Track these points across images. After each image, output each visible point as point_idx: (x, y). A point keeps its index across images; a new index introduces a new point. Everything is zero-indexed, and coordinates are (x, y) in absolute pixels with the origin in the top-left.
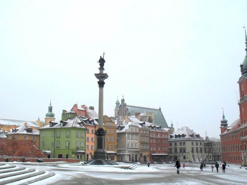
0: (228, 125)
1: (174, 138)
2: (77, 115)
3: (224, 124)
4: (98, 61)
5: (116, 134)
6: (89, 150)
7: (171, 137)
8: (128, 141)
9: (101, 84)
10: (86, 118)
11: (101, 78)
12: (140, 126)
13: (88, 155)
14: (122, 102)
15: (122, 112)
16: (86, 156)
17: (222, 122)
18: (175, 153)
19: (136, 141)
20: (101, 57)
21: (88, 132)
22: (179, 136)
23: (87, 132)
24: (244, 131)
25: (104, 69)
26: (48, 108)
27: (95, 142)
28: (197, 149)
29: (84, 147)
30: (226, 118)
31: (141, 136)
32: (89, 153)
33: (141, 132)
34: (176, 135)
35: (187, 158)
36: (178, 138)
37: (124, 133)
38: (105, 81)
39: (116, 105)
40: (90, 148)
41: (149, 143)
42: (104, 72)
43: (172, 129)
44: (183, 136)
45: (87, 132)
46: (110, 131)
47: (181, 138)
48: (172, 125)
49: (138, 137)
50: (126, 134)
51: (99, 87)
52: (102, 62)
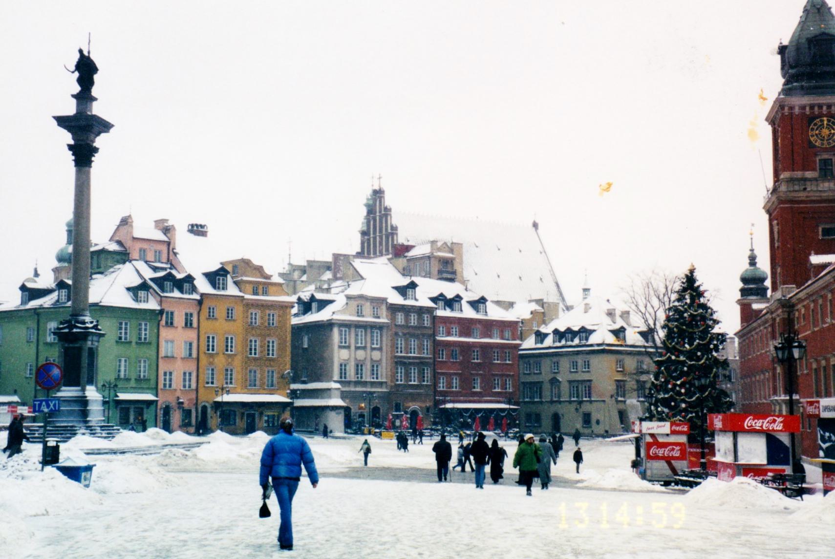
1: (549, 341)
2: (132, 256)
4: (73, 68)
5: (289, 330)
6: (175, 390)
8: (344, 354)
9: (83, 154)
11: (83, 132)
14: (375, 200)
16: (160, 413)
17: (744, 280)
18: (552, 402)
19: (376, 355)
20: (81, 51)
21: (170, 324)
22: (569, 334)
23: (163, 322)
25: (96, 99)
26: (66, 228)
29: (153, 377)
32: (174, 404)
33: (400, 318)
34: (556, 332)
35: (598, 422)
36: (563, 342)
37: (329, 325)
38: (100, 141)
41: (431, 361)
42: (97, 109)
44: (585, 332)
45: (163, 322)
46: (262, 318)
47: (576, 341)
49: (384, 339)
50: (331, 330)
51: (73, 163)
52: (86, 69)
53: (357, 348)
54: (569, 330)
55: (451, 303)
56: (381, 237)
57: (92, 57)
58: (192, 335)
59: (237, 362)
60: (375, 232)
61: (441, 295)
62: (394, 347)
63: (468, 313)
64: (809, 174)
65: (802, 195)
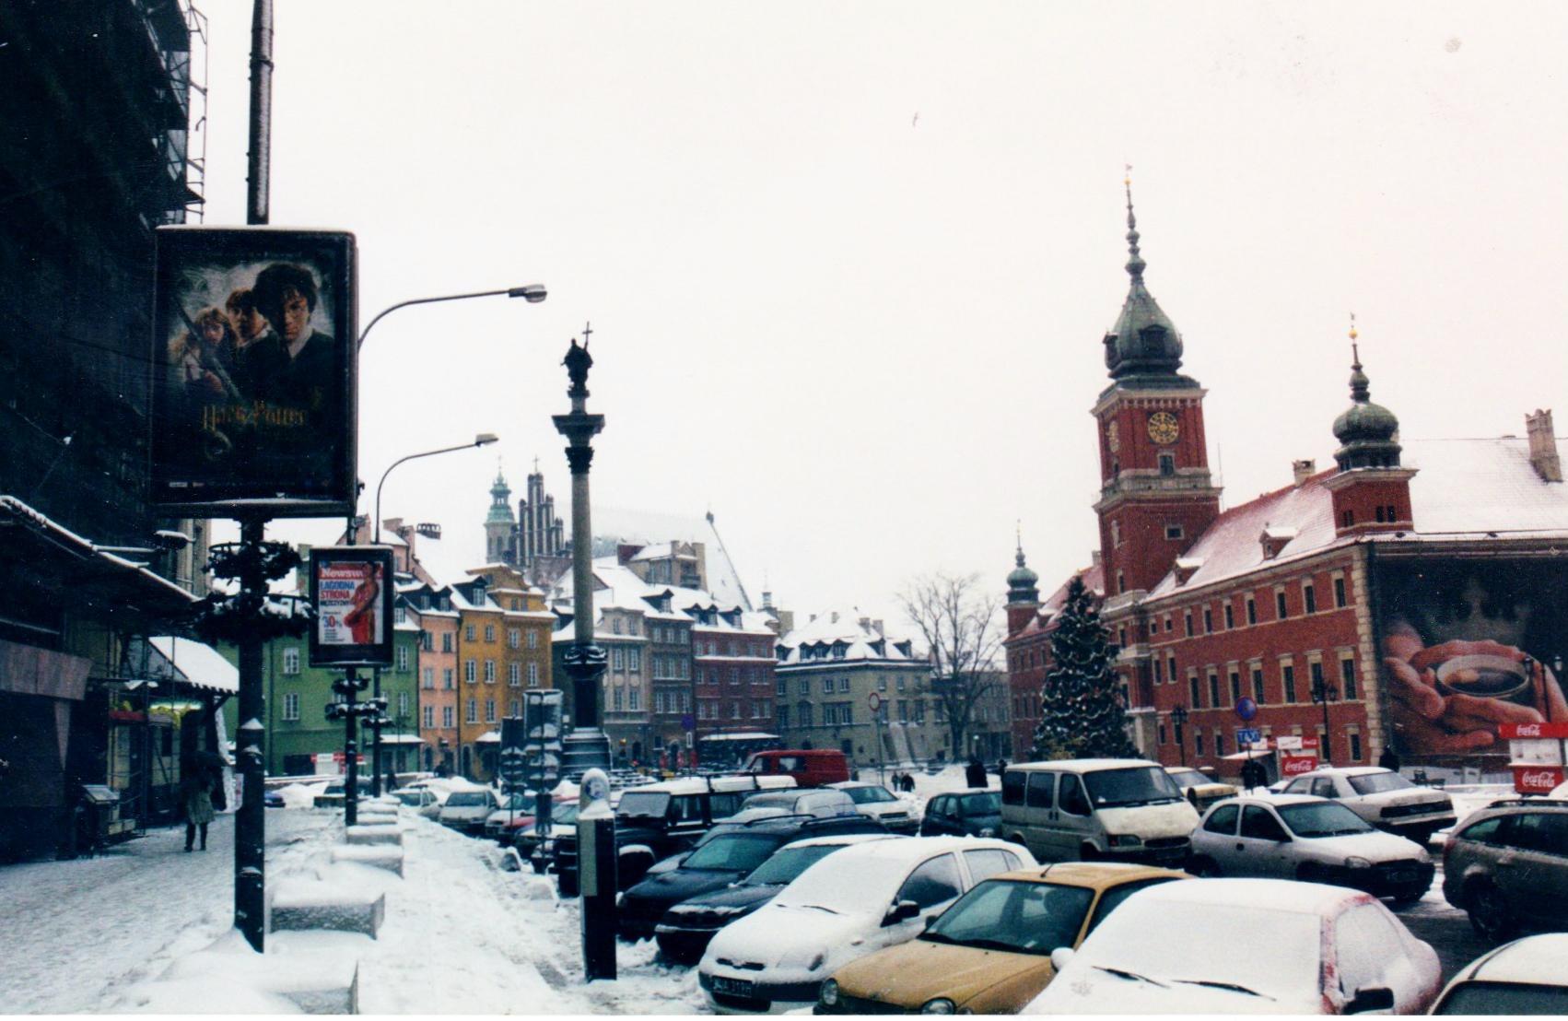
0: (1042, 597)
3: (1023, 587)
5: (549, 649)
7: (784, 652)
9: (580, 459)
10: (409, 581)
12: (651, 612)
13: (429, 752)
15: (531, 536)
16: (423, 757)
17: (1013, 582)
18: (801, 730)
19: (635, 680)
21: (428, 649)
22: (821, 648)
24: (1121, 627)
27: (459, 689)
28: (902, 704)
30: (1031, 565)
31: (655, 654)
34: (804, 646)
35: (861, 750)
36: (813, 658)
39: (490, 500)
40: (438, 719)
42: (591, 407)
43: (782, 622)
44: (841, 646)
47: (830, 657)
48: (766, 595)
52: (578, 362)
53: (616, 672)
54: (820, 644)
55: (706, 615)
56: (540, 535)
57: (590, 351)
58: (450, 661)
59: (499, 695)
60: (531, 527)
61: (697, 606)
62: (652, 670)
63: (723, 627)
64: (1151, 472)
65: (1149, 494)
